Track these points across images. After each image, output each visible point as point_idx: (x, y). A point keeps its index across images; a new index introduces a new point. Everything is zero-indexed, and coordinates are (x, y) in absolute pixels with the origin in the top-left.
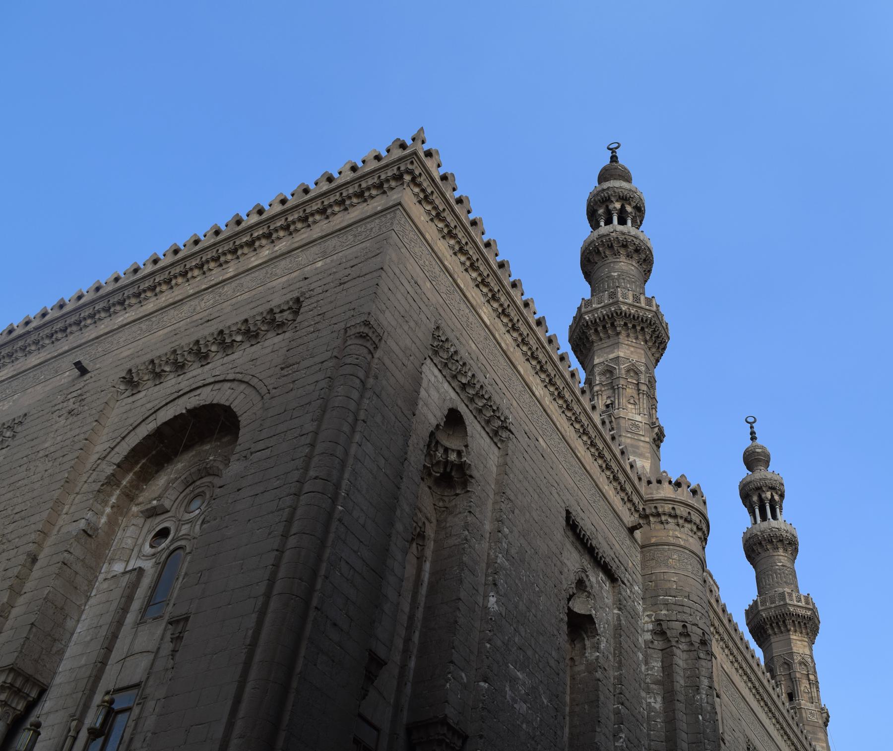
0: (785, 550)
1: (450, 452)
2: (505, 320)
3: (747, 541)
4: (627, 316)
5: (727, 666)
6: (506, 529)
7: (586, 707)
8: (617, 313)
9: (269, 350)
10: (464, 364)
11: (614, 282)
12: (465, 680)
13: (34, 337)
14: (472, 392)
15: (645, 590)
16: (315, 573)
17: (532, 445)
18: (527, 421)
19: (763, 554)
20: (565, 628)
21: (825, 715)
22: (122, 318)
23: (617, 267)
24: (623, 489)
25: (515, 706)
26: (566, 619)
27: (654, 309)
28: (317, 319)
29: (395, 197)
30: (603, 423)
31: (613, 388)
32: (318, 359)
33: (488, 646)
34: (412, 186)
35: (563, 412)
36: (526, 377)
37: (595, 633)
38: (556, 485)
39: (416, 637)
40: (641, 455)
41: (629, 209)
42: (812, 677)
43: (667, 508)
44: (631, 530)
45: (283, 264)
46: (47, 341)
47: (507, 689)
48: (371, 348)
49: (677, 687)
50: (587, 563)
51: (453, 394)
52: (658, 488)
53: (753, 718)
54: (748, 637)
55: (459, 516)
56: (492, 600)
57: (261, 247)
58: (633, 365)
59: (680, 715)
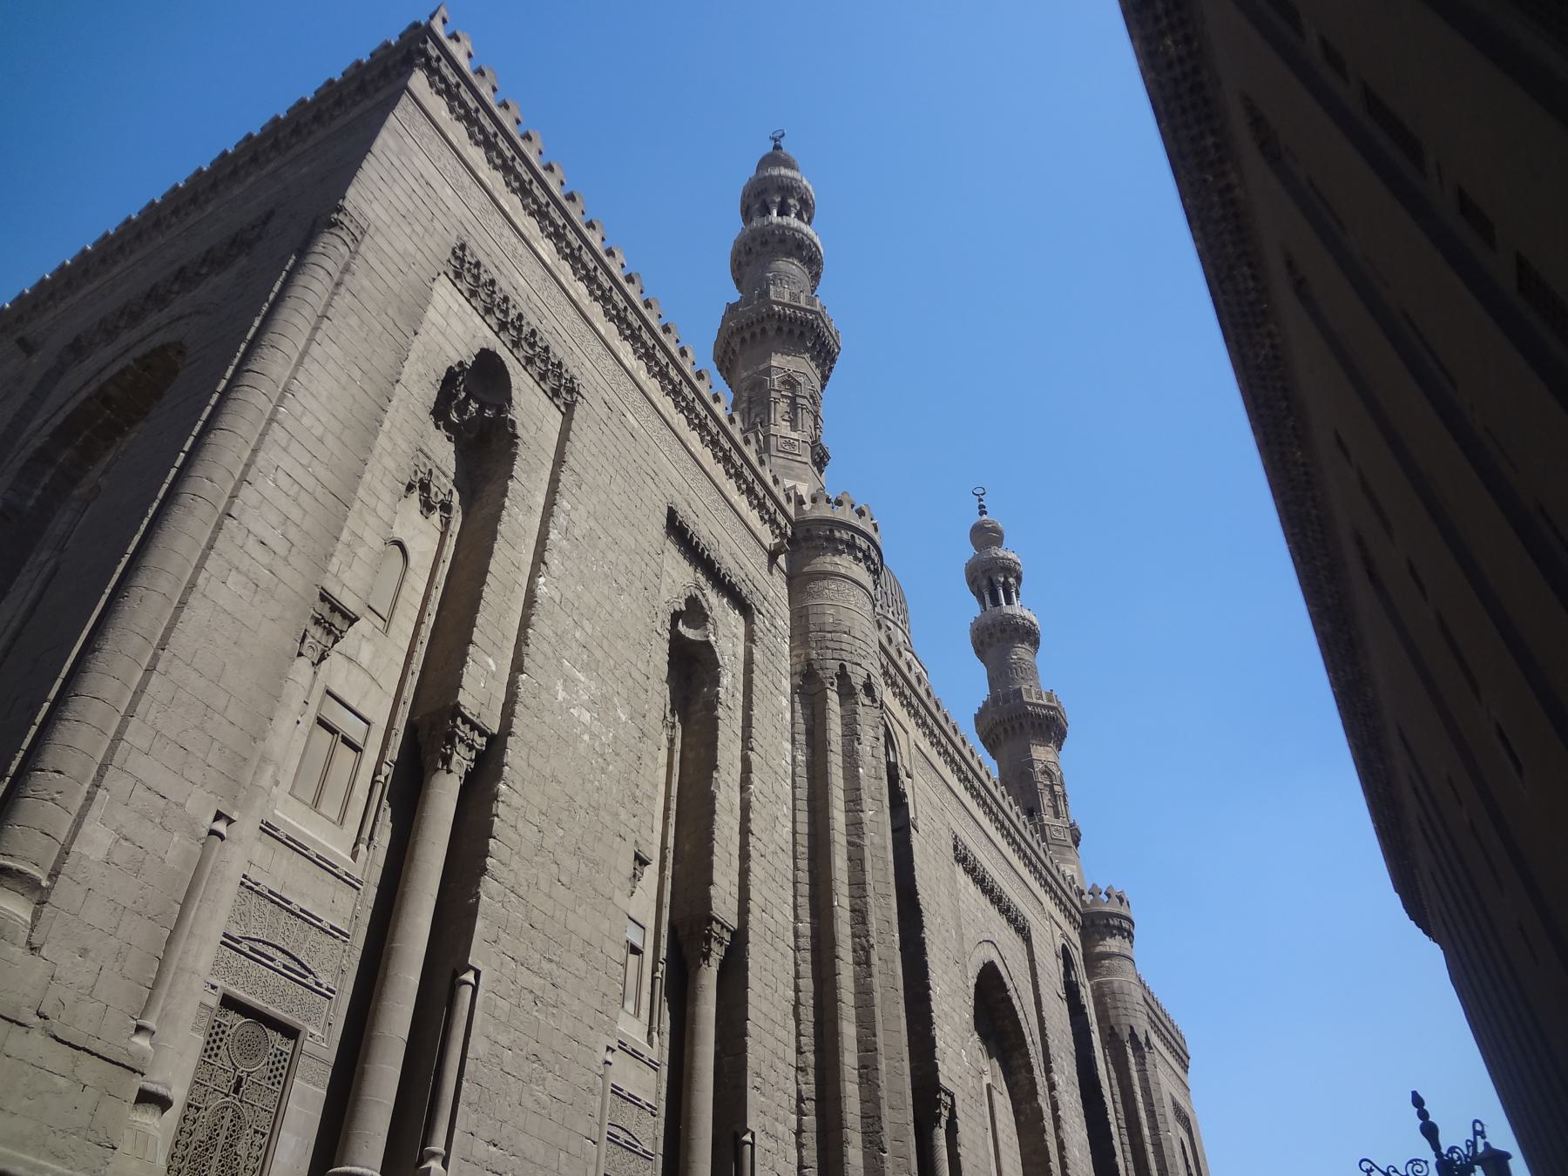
4: (781, 318)
5: (925, 745)
20: (667, 646)
41: (791, 201)
42: (1056, 788)
47: (559, 687)
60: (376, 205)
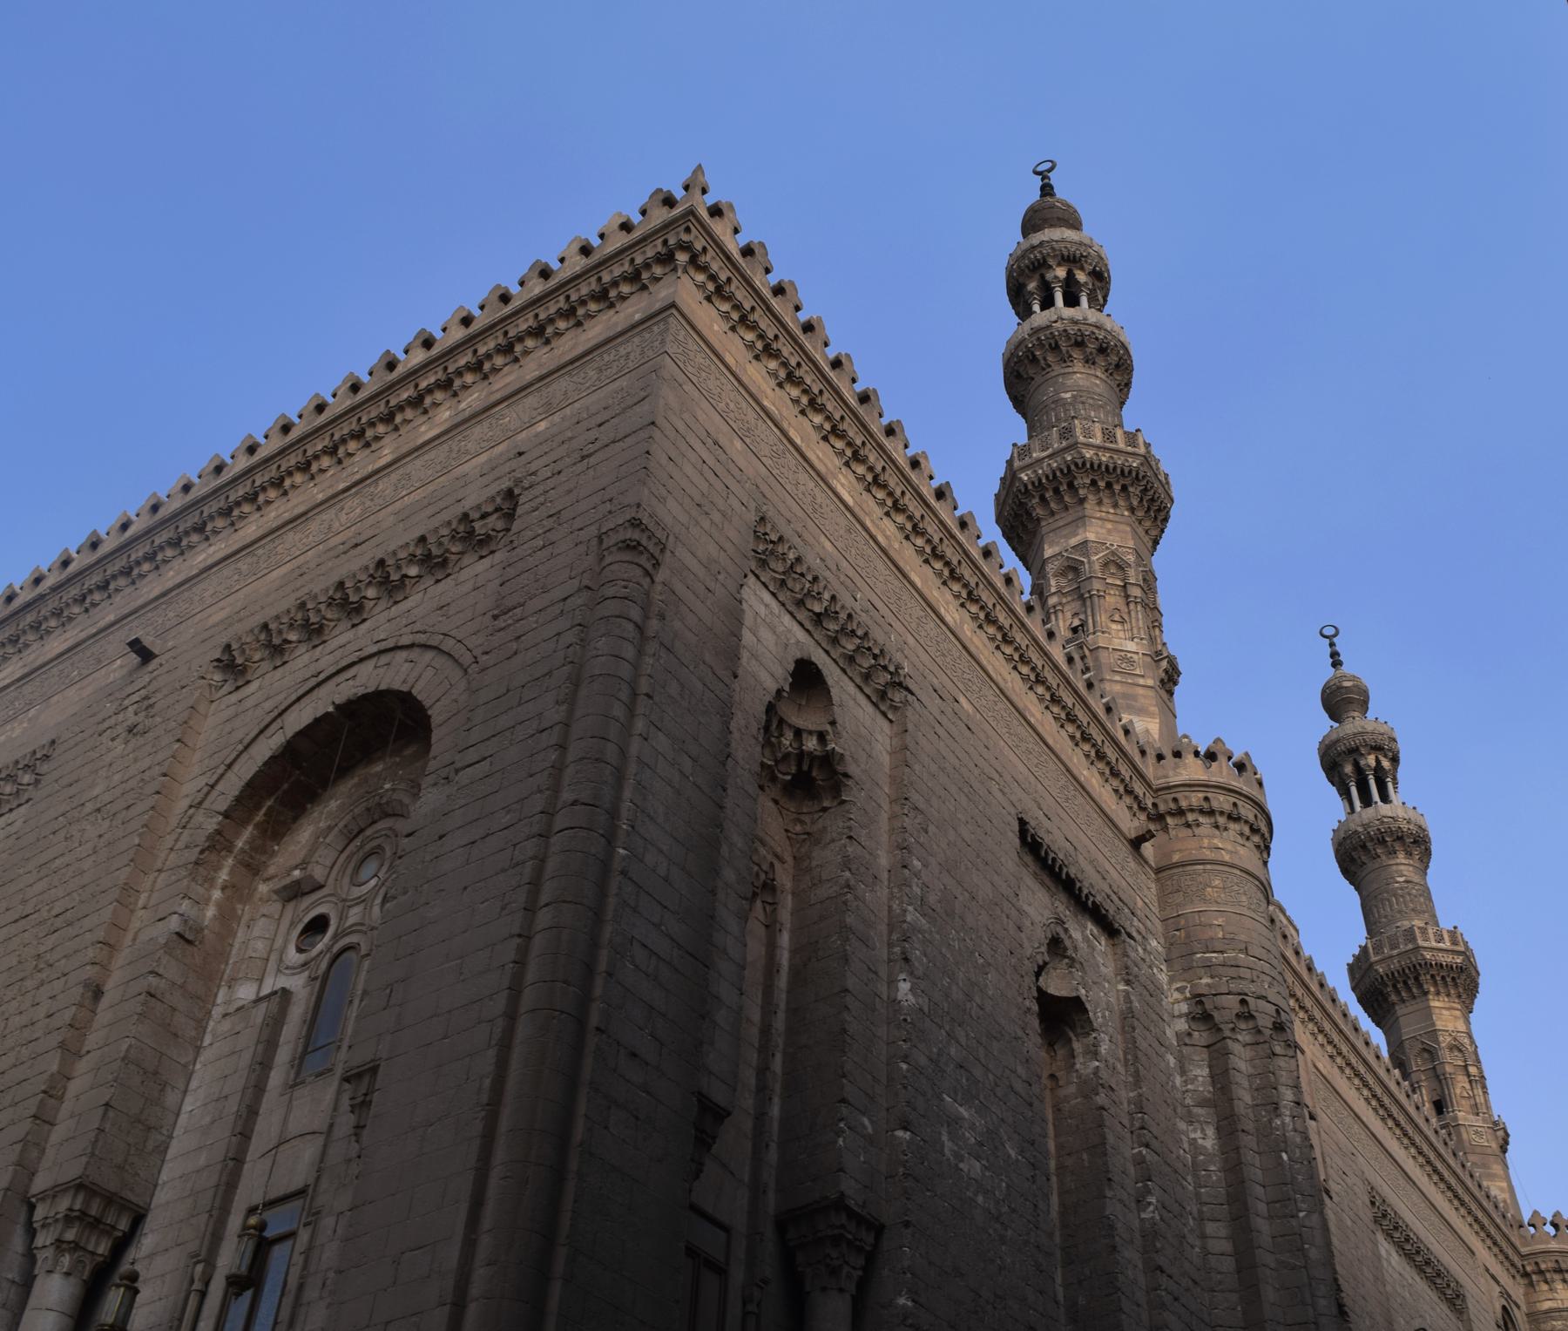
0: (1409, 854)
1: (805, 736)
2: (880, 495)
3: (1340, 844)
4: (1094, 468)
5: (1325, 1065)
6: (916, 862)
7: (1085, 1156)
8: (1076, 465)
9: (469, 586)
10: (816, 579)
11: (1066, 411)
12: (870, 1130)
13: (52, 604)
14: (833, 626)
15: (1170, 945)
16: (589, 969)
17: (949, 711)
18: (936, 669)
19: (1370, 865)
20: (1036, 1023)
21: (1501, 1133)
22: (204, 555)
23: (1069, 382)
24: (1115, 774)
25: (961, 1165)
26: (1036, 1008)
27: (1142, 450)
28: (548, 523)
29: (663, 294)
30: (1070, 660)
31: (1081, 597)
32: (558, 593)
33: (904, 1066)
34: (692, 272)
35: (998, 648)
36: (925, 591)
37: (1088, 1027)
38: (996, 777)
39: (777, 1064)
40: (1142, 711)
41: (1081, 277)
42: (1472, 1070)
43: (1196, 799)
44: (1136, 843)
45: (478, 431)
46: (76, 610)
47: (945, 1138)
48: (649, 566)
49: (1240, 1108)
50: (1063, 907)
51: (800, 635)
52: (1177, 766)
53: (1376, 1149)
54: (1357, 1011)
55: (832, 846)
56: (904, 987)
57: (436, 405)
58: (1113, 553)
59: (1250, 1157)
60: (671, 503)
